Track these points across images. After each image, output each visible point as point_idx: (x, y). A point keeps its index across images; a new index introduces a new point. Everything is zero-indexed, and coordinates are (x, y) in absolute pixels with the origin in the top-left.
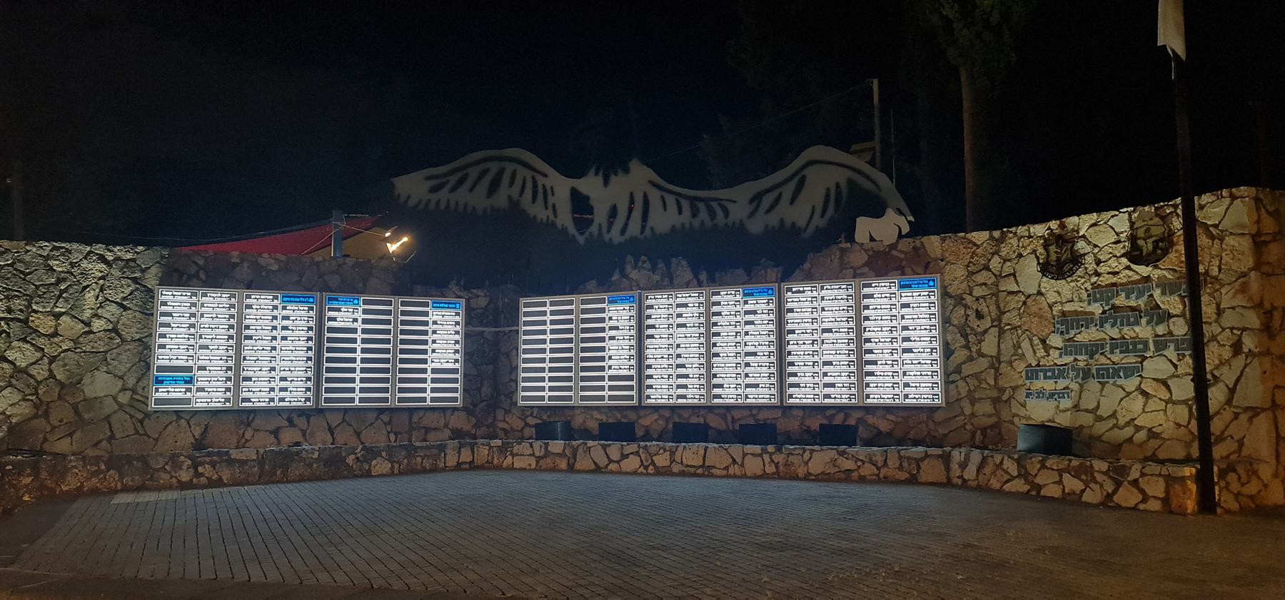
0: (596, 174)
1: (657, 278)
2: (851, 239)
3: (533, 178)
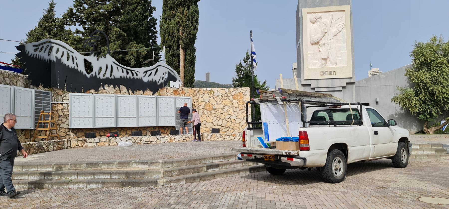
0: (94, 56)
2: (169, 86)
3: (67, 52)
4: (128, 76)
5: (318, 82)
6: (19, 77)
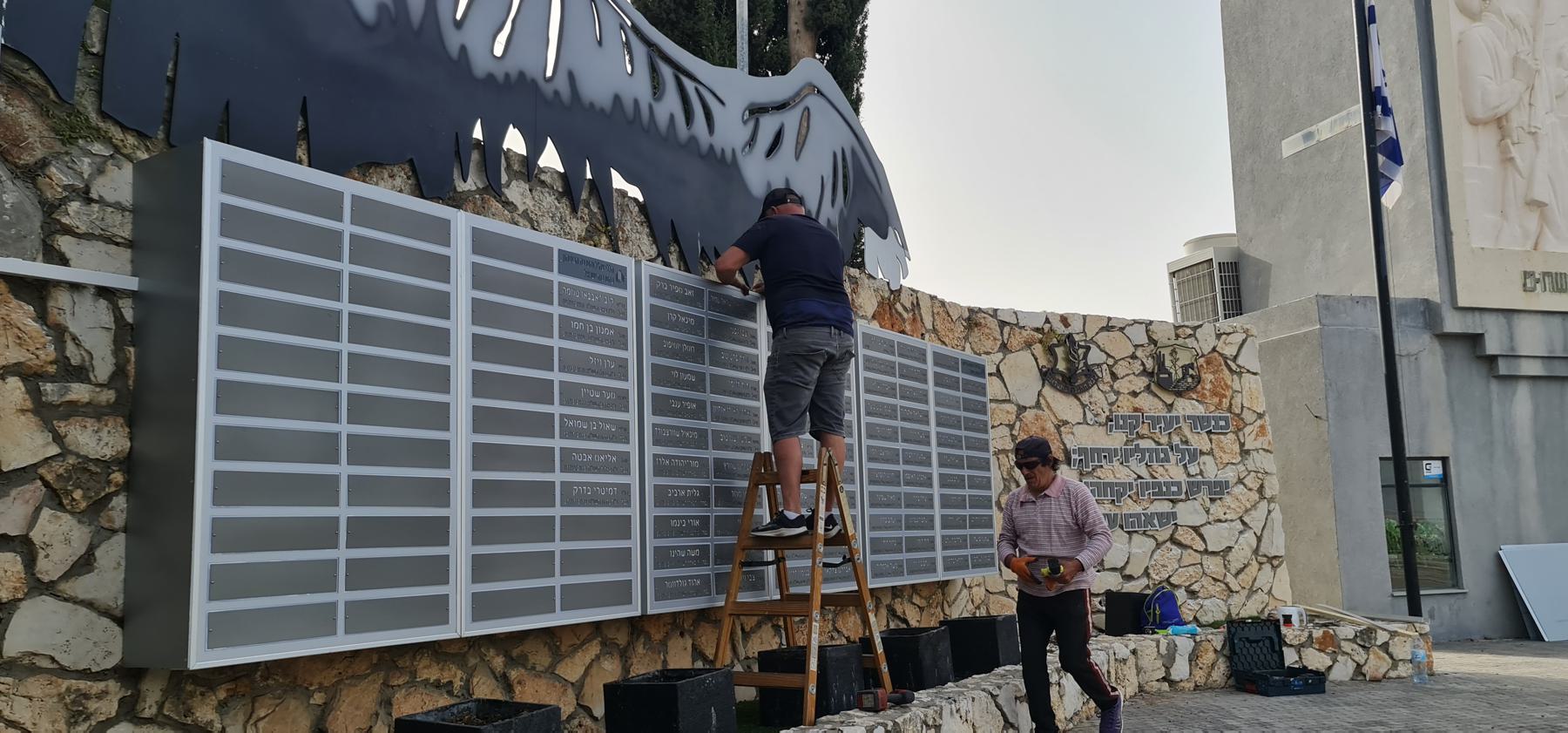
2: (861, 266)
5: (1510, 327)
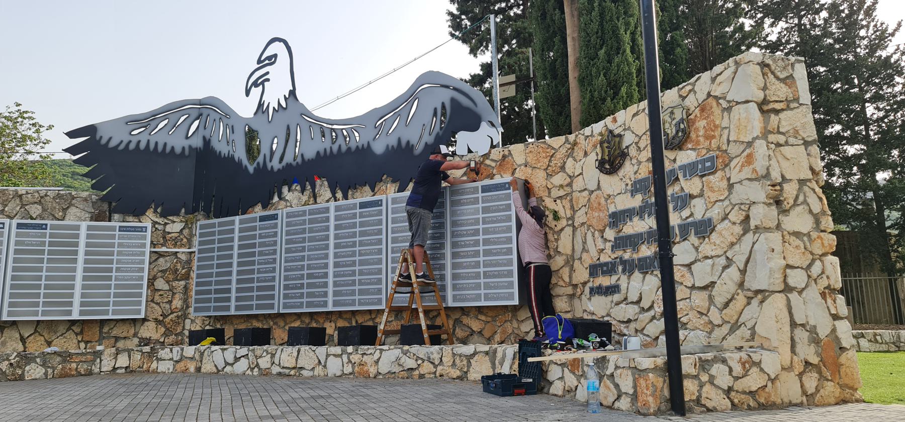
1: (305, 198)
4: (335, 148)
6: (73, 198)
